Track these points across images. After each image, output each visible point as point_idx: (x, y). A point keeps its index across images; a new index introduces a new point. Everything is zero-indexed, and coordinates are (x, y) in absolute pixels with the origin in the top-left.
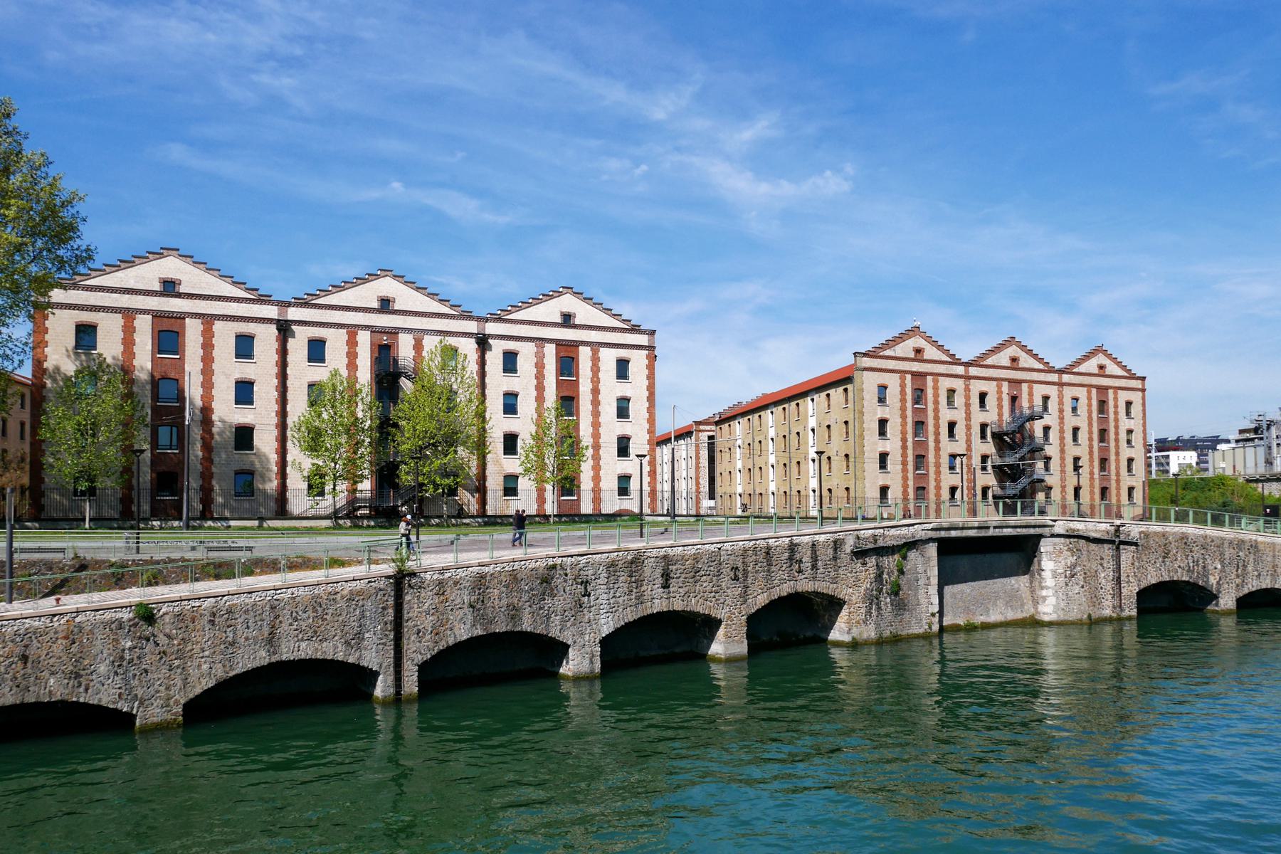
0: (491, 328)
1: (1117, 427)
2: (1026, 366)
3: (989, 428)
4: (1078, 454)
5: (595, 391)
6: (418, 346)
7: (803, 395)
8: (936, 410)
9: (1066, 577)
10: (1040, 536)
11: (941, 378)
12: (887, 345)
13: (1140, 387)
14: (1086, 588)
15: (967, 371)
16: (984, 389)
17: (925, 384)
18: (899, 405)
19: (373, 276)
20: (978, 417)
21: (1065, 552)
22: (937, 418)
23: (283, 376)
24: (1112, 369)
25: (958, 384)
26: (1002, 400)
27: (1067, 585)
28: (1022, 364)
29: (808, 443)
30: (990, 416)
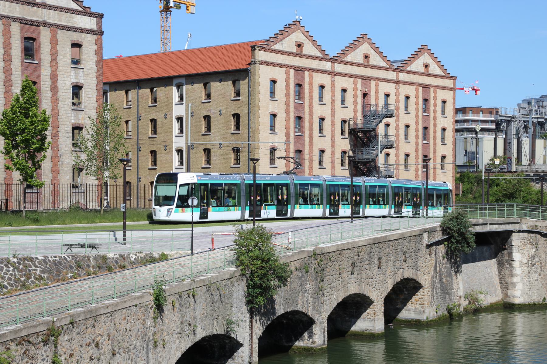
1: (435, 126)
2: (375, 64)
3: (347, 124)
4: (408, 151)
5: (54, 77)
7: (166, 81)
8: (311, 106)
9: (528, 266)
10: (511, 232)
11: (315, 74)
12: (278, 37)
13: (452, 86)
14: (542, 276)
15: (333, 67)
16: (345, 86)
17: (303, 80)
18: (284, 99)
20: (343, 114)
21: (528, 245)
22: (311, 114)
24: (434, 69)
25: (325, 80)
26: (357, 96)
27: (529, 273)
28: (372, 62)
29: (171, 133)
30: (348, 114)
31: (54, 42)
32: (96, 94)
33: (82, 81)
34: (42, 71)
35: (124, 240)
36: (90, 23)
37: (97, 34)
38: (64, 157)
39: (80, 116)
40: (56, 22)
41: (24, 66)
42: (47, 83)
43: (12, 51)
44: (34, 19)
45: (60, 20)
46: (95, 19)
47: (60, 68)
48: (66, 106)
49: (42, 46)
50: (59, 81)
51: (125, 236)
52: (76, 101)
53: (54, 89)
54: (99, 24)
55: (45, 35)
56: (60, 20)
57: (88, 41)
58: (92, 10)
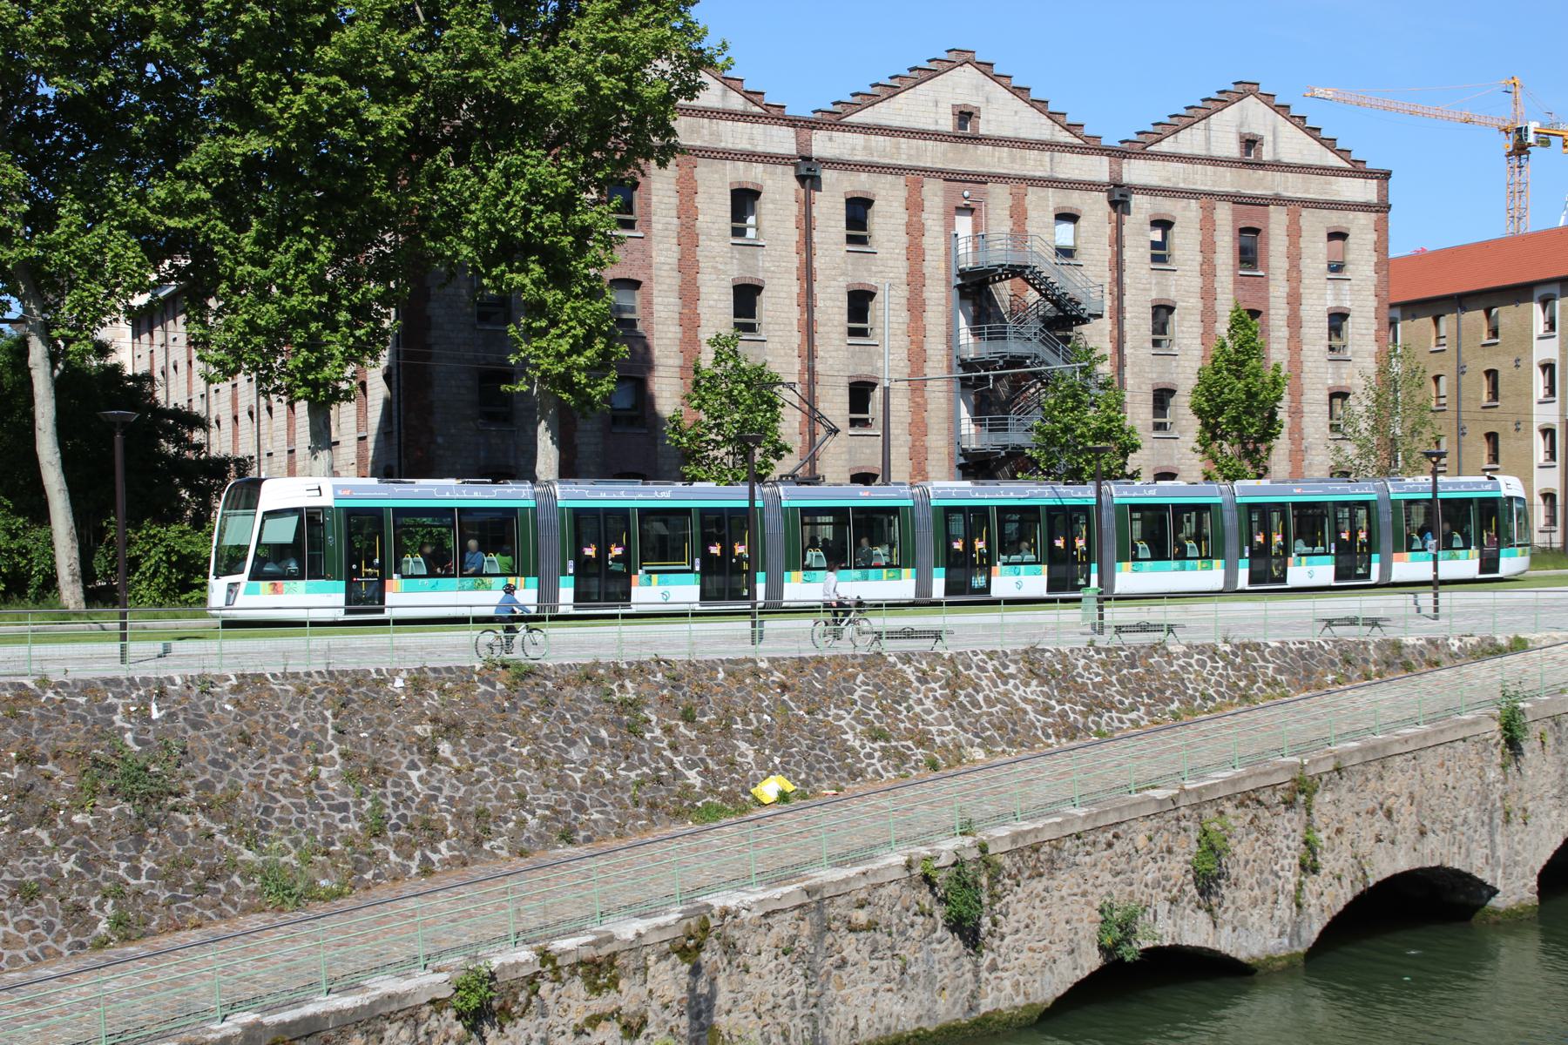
0: (1136, 172)
5: (1294, 300)
6: (1018, 214)
7: (1519, 293)
19: (1223, 100)
23: (808, 274)
29: (1530, 395)
31: (1294, 233)
32: (1375, 327)
33: (1347, 304)
34: (1271, 289)
35: (1436, 610)
36: (1364, 190)
37: (1377, 211)
38: (1313, 452)
39: (1343, 371)
40: (1299, 195)
41: (1239, 281)
42: (1281, 312)
43: (1217, 255)
44: (1258, 192)
45: (1307, 191)
46: (1375, 181)
47: (1305, 281)
48: (1316, 354)
49: (1271, 242)
50: (1302, 307)
51: (1436, 602)
52: (1335, 342)
53: (1295, 322)
54: (1383, 192)
55: (1277, 223)
56: (1307, 191)
57: (1361, 227)
58: (1369, 166)
